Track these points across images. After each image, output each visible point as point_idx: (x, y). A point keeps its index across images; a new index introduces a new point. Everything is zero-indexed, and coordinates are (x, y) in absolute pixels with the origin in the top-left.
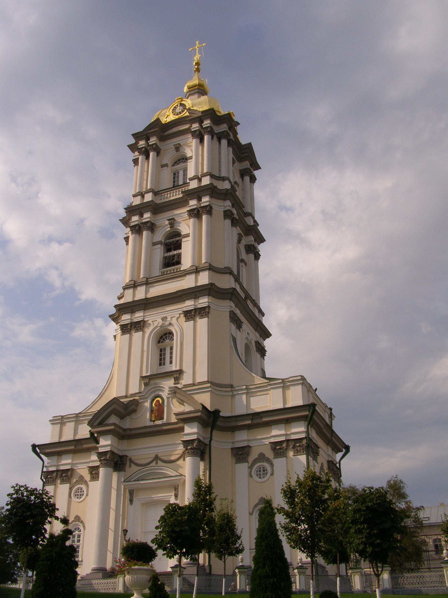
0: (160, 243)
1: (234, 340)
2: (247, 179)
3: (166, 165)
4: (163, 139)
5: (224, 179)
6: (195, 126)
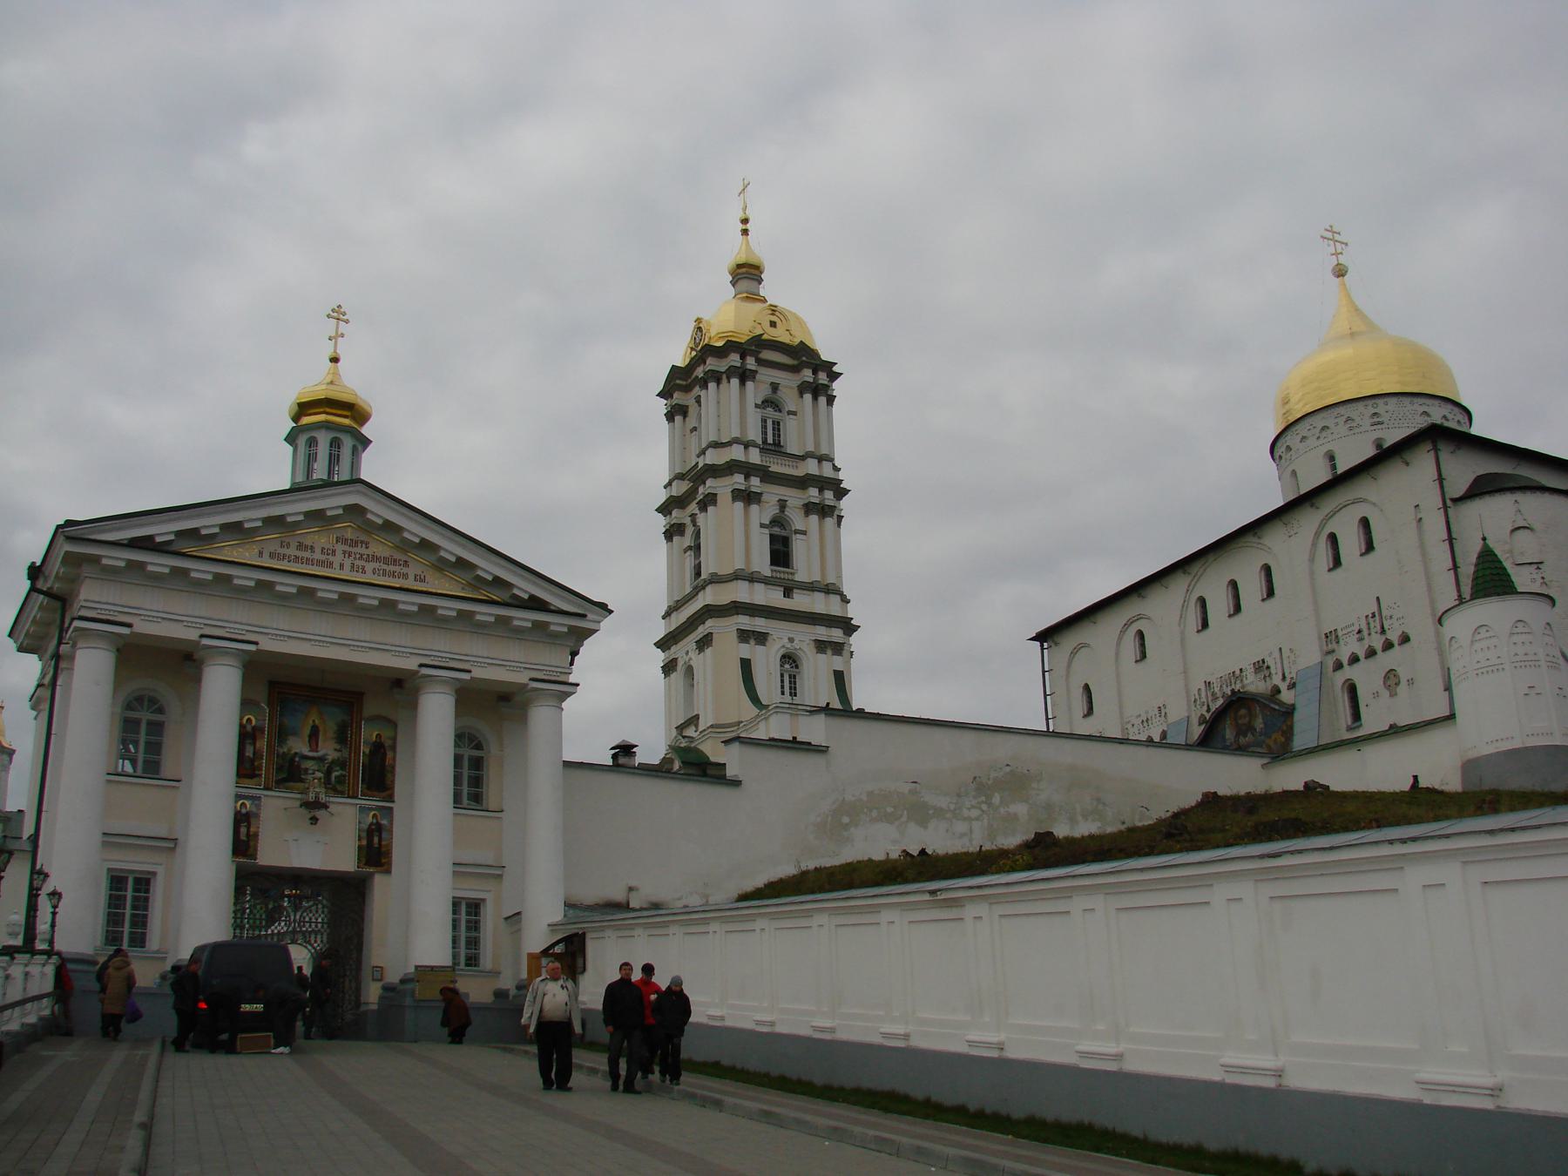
0: (690, 548)
1: (746, 665)
2: (808, 397)
3: (695, 429)
4: (687, 389)
5: (729, 444)
6: (699, 372)
